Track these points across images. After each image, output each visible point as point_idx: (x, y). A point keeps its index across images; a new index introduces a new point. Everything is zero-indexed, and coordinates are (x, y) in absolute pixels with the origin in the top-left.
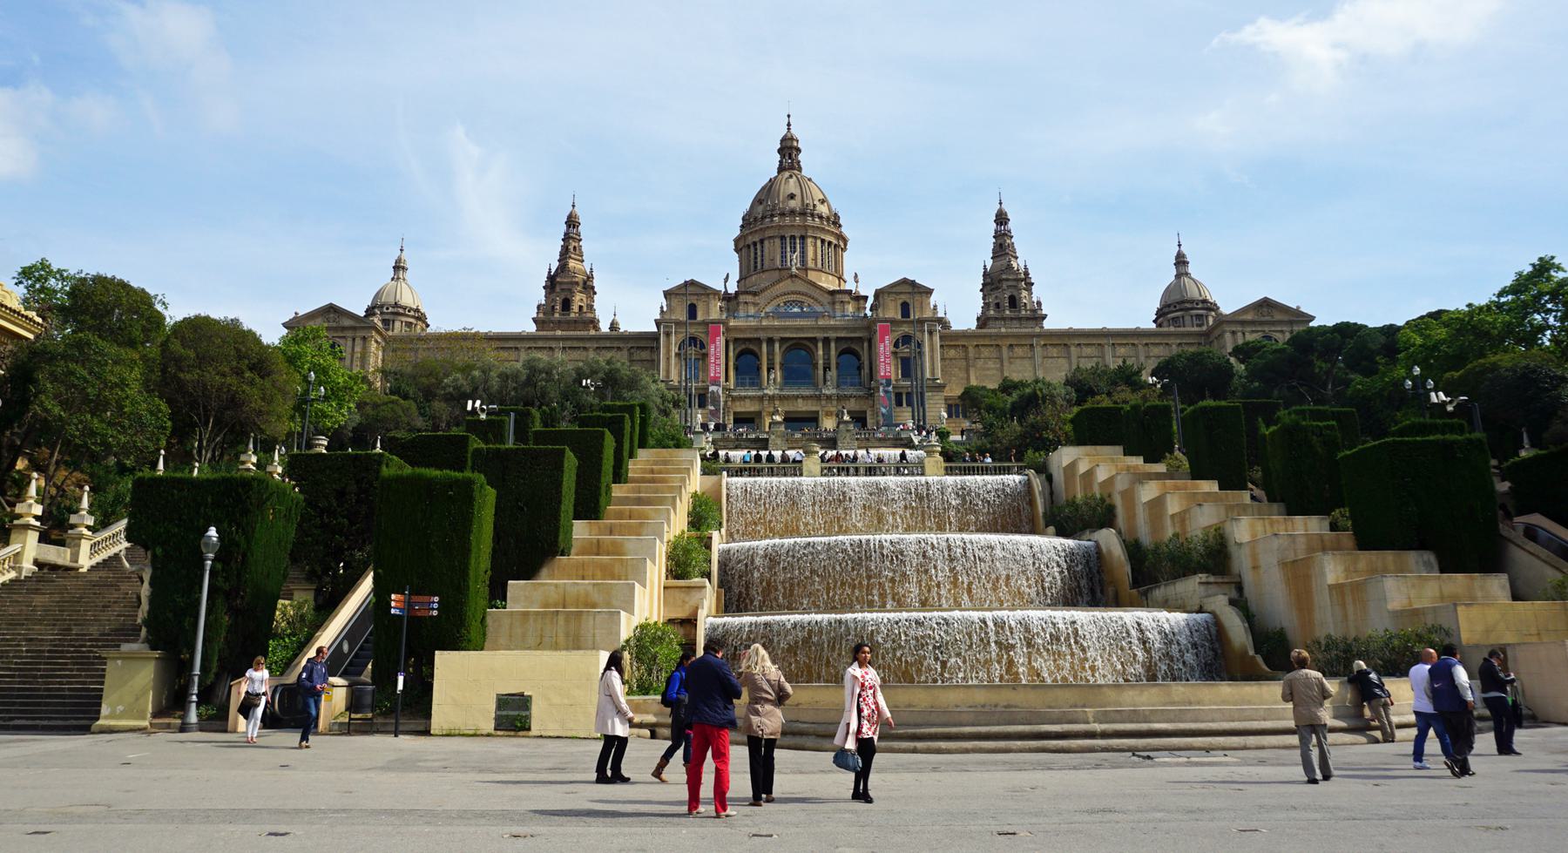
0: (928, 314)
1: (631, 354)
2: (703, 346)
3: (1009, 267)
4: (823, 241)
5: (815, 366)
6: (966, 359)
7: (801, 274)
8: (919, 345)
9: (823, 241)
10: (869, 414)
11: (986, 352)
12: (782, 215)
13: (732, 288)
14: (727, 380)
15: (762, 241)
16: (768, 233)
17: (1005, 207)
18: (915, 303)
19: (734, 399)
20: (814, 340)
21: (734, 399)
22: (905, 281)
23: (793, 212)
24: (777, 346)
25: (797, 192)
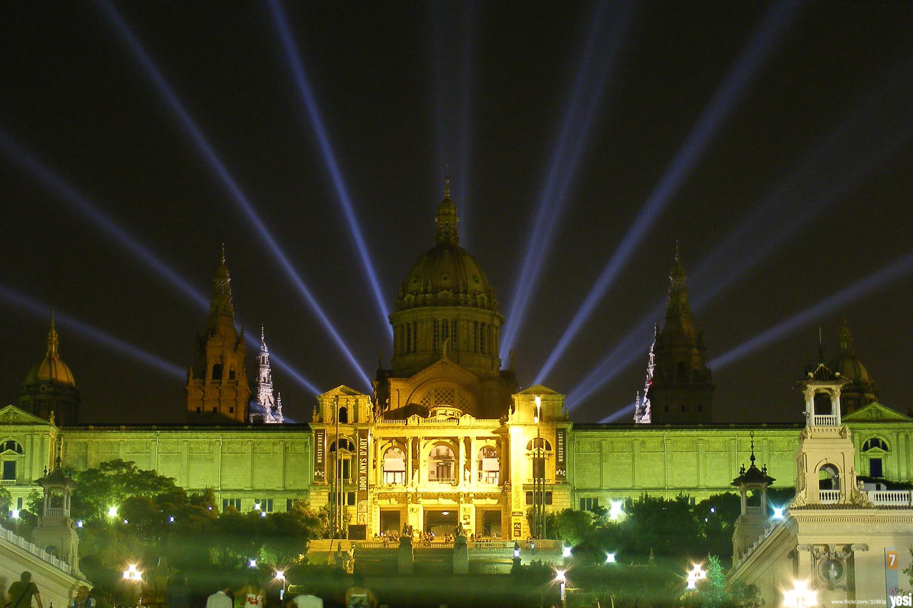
2: (352, 448)
4: (476, 323)
8: (548, 448)
9: (476, 323)
15: (415, 323)
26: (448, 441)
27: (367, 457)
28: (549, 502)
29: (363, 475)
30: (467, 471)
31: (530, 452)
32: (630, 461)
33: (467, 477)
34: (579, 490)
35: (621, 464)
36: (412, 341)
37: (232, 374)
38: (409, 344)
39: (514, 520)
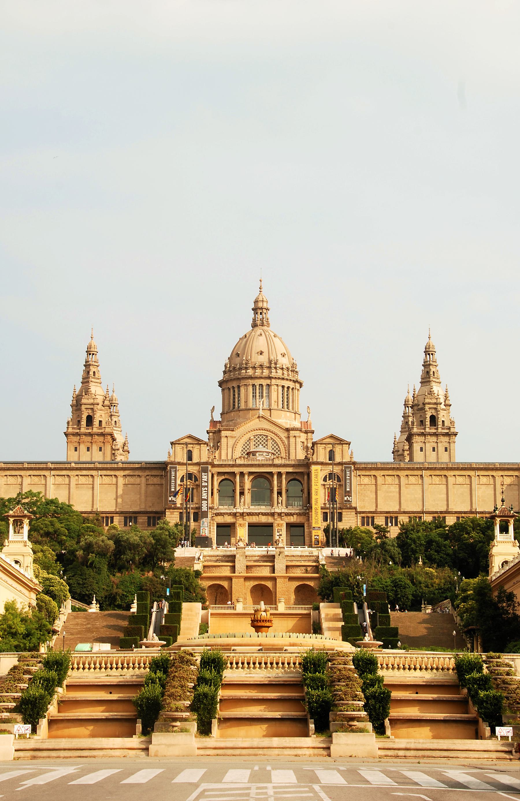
0: (346, 459)
1: (147, 480)
2: (196, 479)
3: (431, 393)
4: (283, 387)
5: (272, 491)
6: (376, 485)
7: (267, 414)
9: (283, 387)
10: (306, 525)
11: (389, 479)
12: (254, 368)
13: (217, 417)
14: (213, 503)
15: (239, 387)
16: (243, 382)
17: (433, 342)
18: (338, 449)
19: (217, 514)
20: (271, 474)
21: (217, 514)
22: (332, 437)
23: (261, 366)
24: (246, 477)
25: (265, 350)
26: (265, 475)
27: (207, 486)
28: (340, 520)
29: (205, 500)
30: (280, 498)
31: (326, 483)
32: (398, 490)
33: (280, 501)
34: (360, 513)
35: (391, 492)
36: (236, 400)
37: (100, 422)
38: (234, 402)
39: (314, 533)
